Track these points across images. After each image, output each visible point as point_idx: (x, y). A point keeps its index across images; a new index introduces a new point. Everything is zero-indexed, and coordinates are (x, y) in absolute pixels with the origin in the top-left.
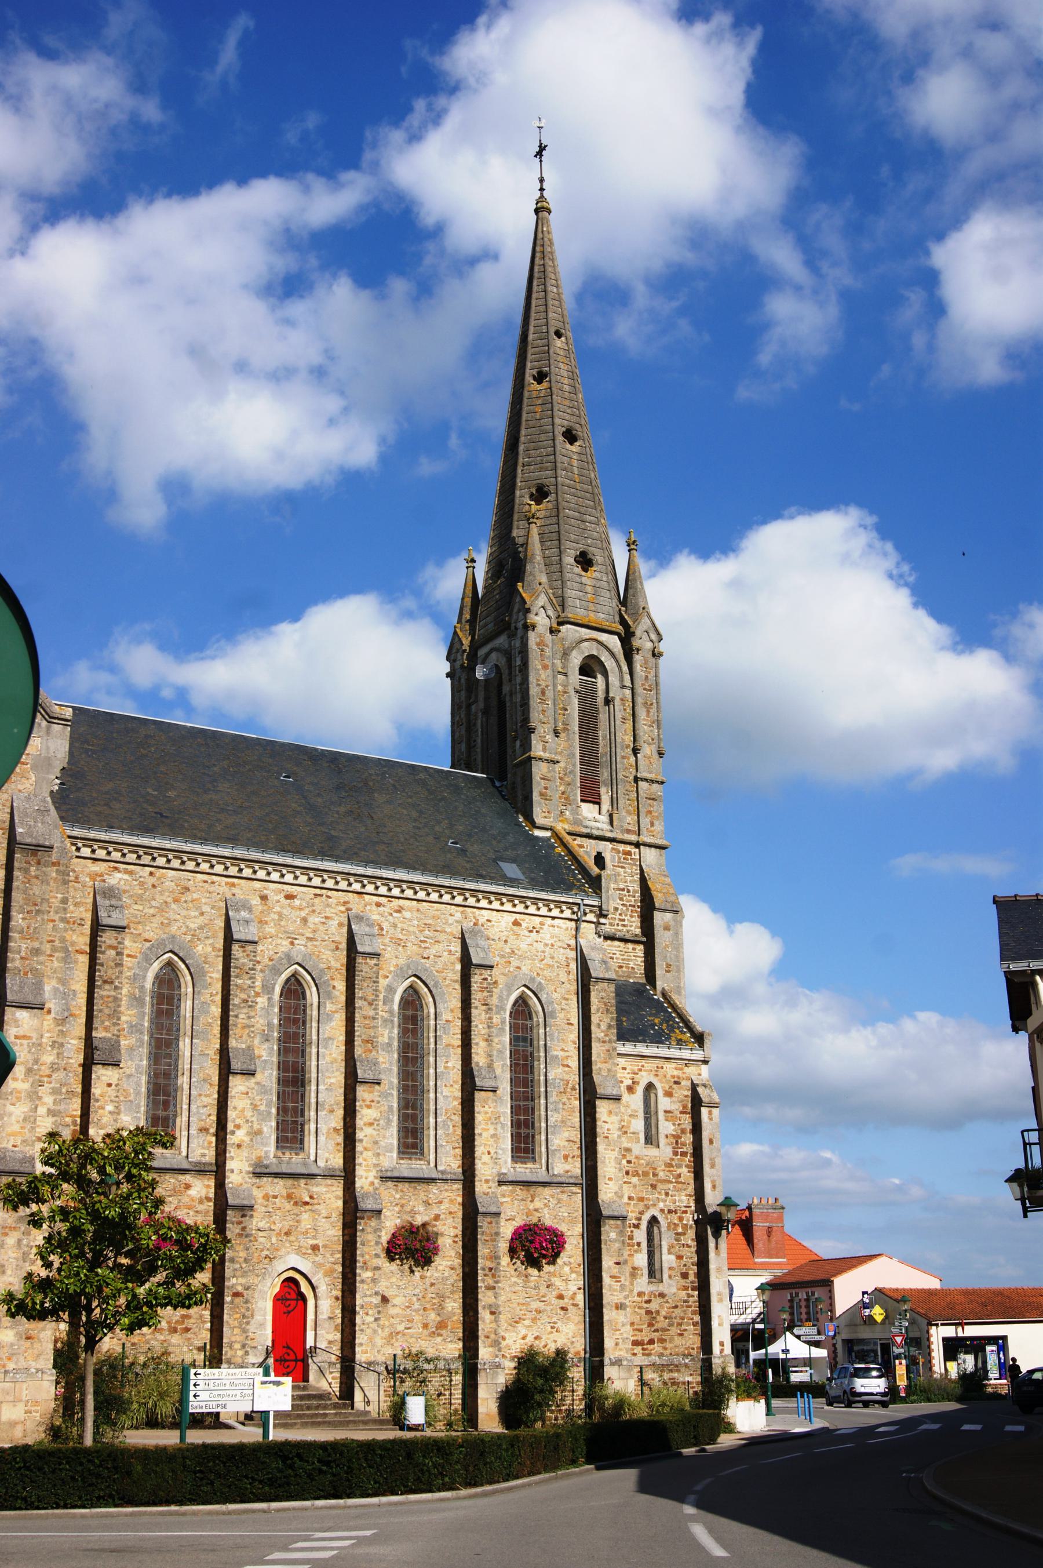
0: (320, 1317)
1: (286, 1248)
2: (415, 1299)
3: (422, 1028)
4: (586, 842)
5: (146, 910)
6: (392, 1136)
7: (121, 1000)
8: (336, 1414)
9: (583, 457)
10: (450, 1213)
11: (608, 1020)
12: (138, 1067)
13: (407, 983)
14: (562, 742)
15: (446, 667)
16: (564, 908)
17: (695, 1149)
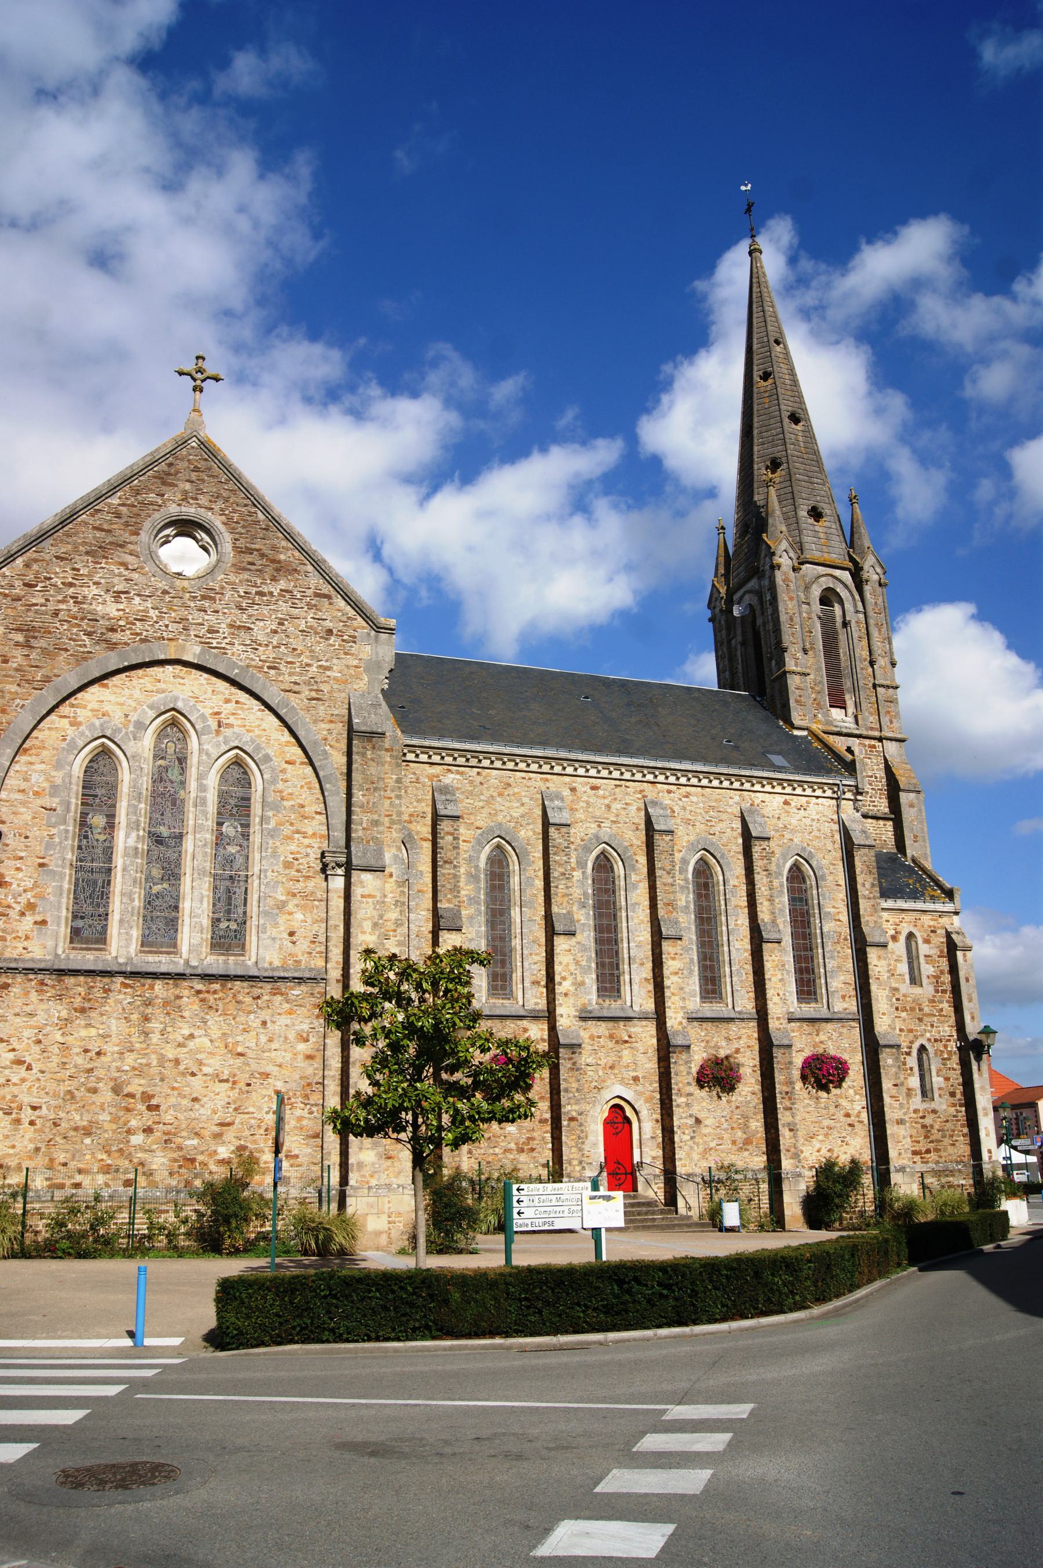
0: (644, 1137)
2: (723, 1120)
4: (837, 738)
5: (476, 804)
6: (694, 984)
7: (460, 877)
8: (663, 1219)
9: (807, 434)
11: (871, 880)
12: (478, 932)
13: (698, 856)
14: (810, 659)
15: (708, 614)
16: (826, 788)
17: (953, 987)
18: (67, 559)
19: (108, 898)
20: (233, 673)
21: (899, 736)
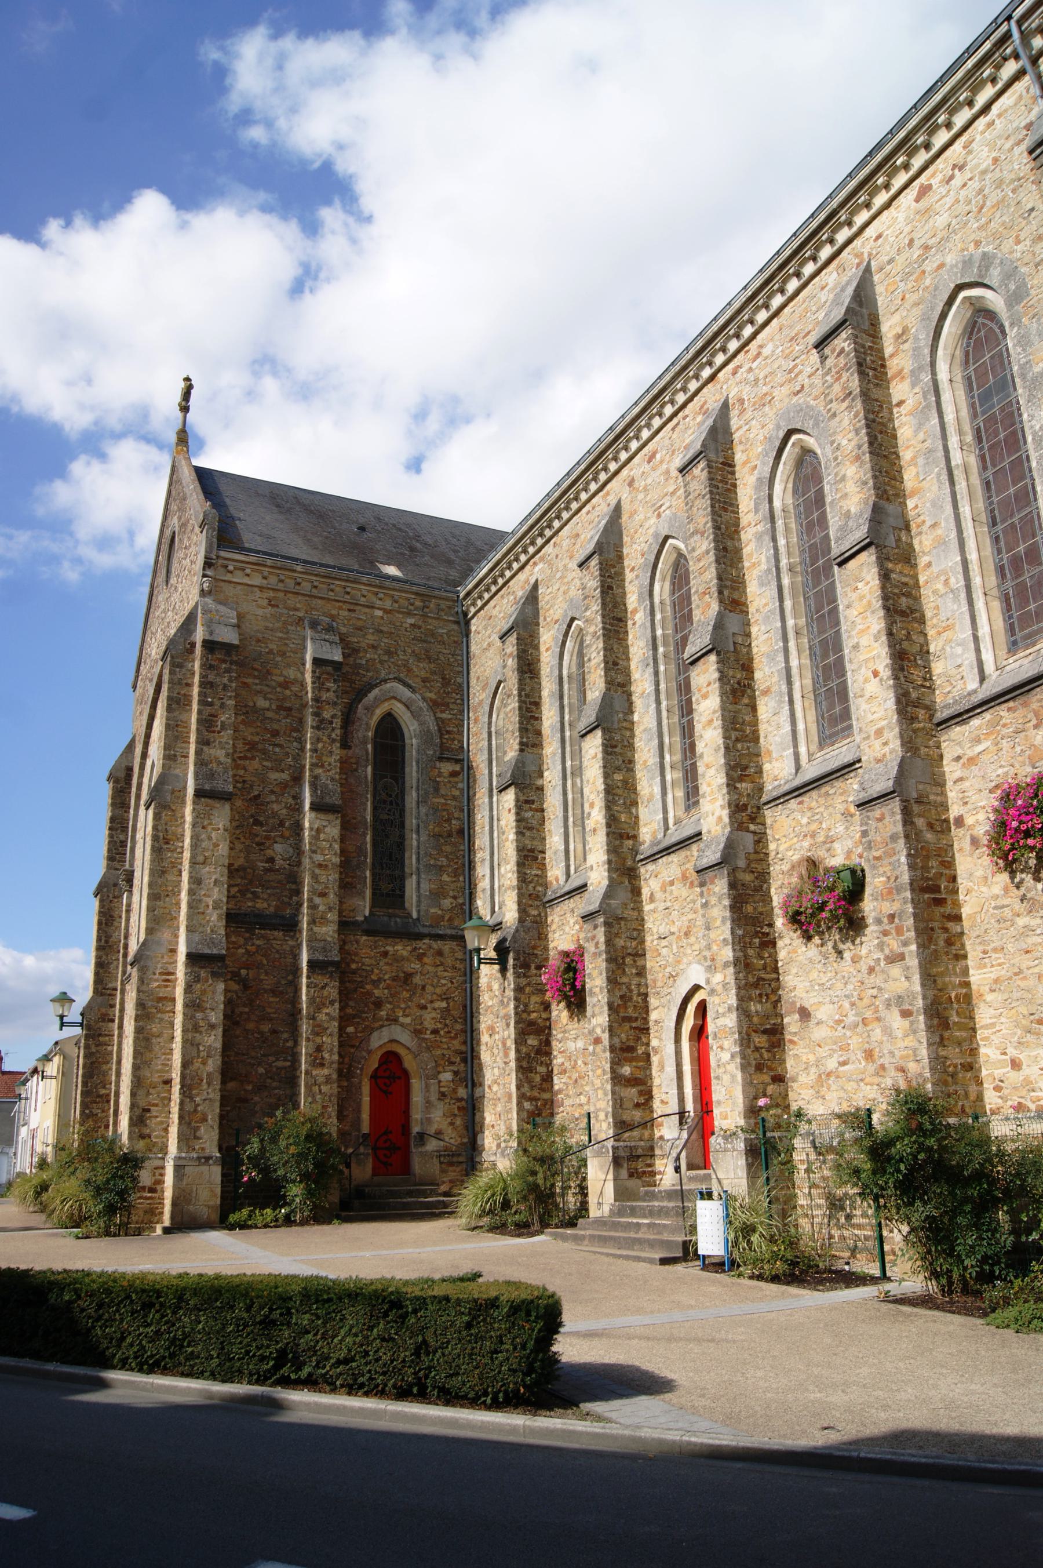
2: (846, 1005)
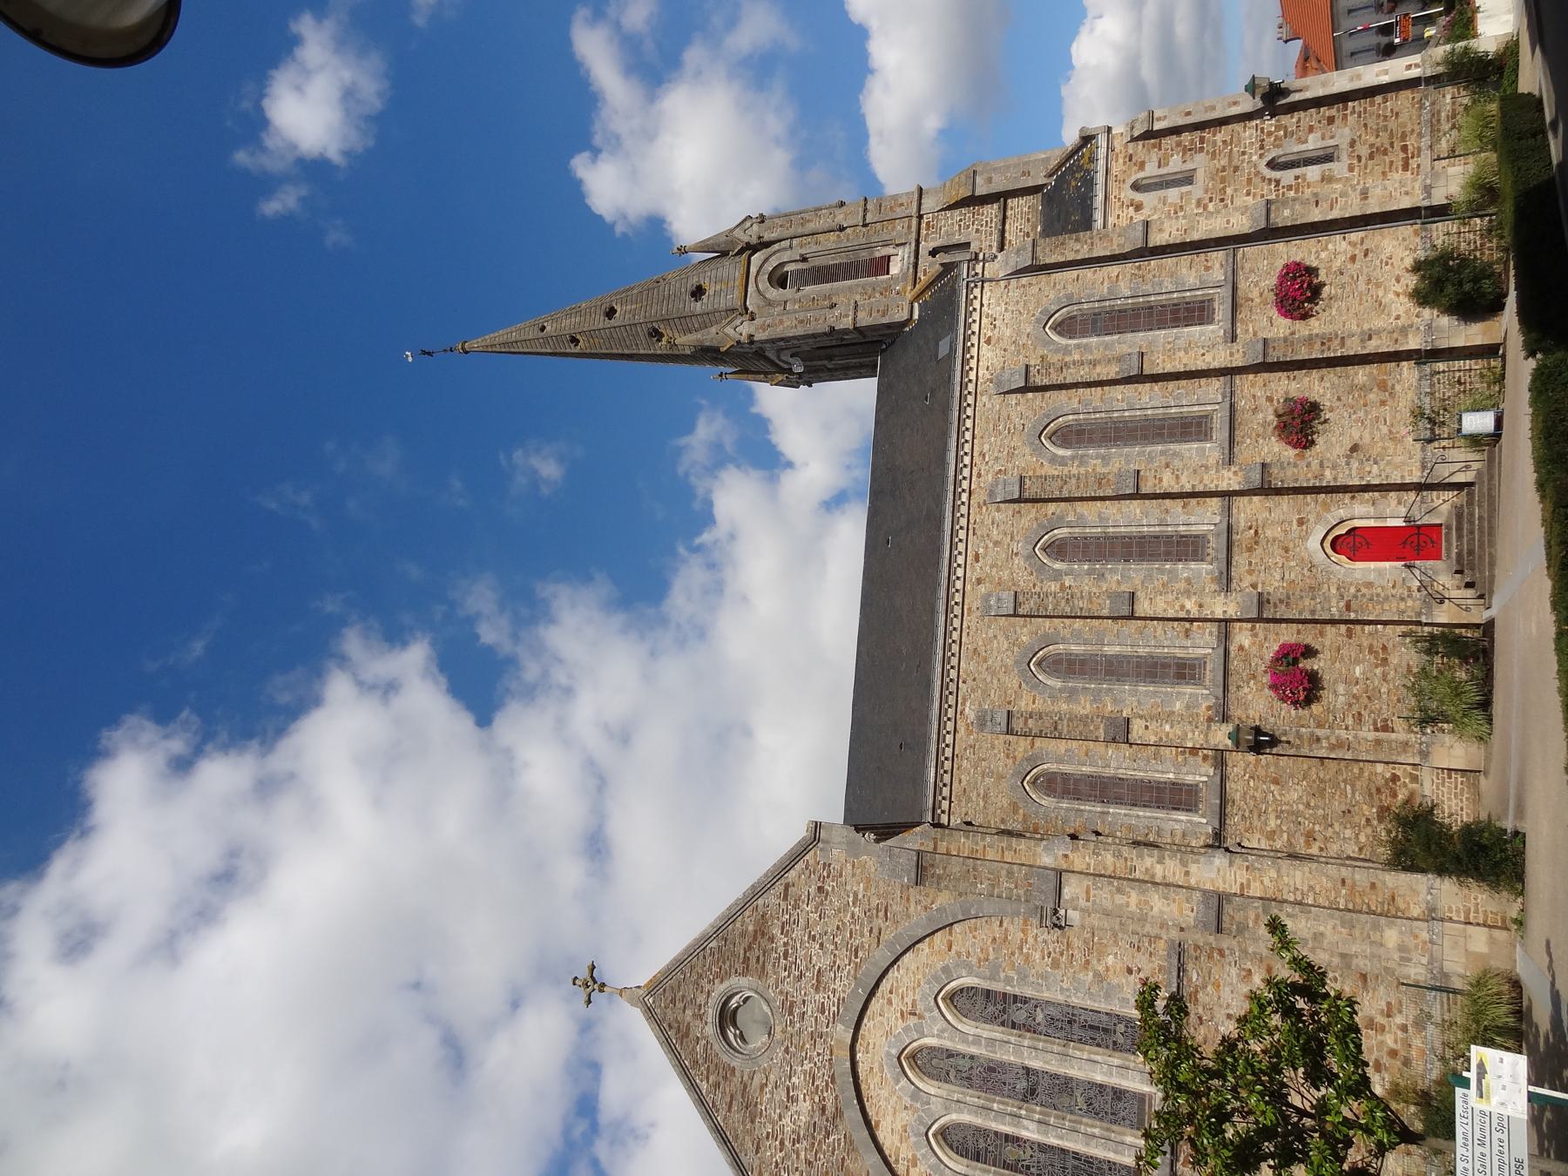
1: (1299, 554)
2: (1354, 417)
3: (1087, 425)
4: (921, 267)
6: (1189, 449)
9: (624, 301)
10: (1265, 385)
17: (1196, 129)
18: (758, 1143)
19: (1092, 1157)
20: (862, 994)
21: (916, 196)
